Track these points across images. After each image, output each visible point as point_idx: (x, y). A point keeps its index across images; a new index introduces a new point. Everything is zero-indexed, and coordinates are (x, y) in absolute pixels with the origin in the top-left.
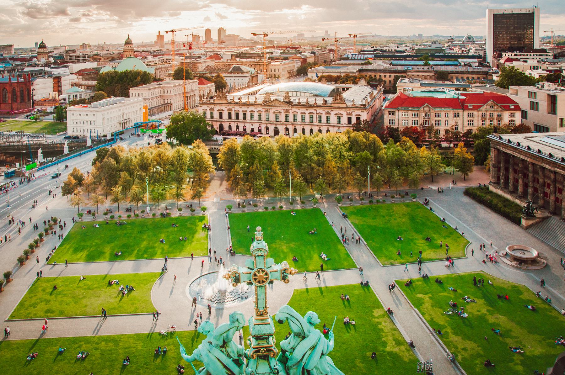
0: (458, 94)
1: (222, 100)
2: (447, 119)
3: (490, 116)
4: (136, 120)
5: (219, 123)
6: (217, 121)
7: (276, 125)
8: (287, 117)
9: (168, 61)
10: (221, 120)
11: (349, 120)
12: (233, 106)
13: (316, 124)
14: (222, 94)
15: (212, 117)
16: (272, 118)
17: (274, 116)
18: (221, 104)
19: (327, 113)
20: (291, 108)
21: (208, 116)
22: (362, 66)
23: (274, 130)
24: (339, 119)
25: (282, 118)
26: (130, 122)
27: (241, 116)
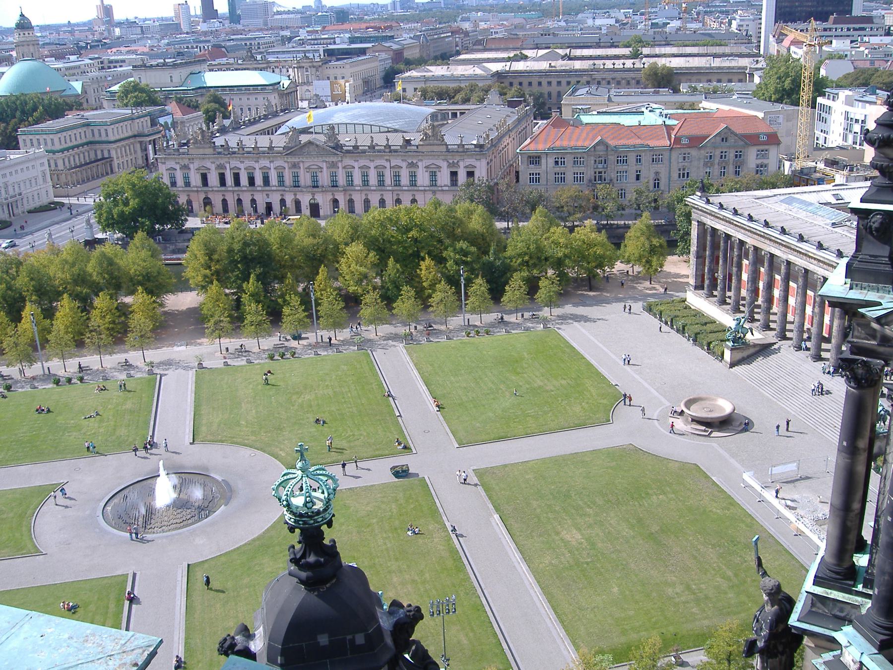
0: (666, 115)
1: (204, 148)
2: (638, 167)
3: (721, 157)
4: (36, 197)
5: (202, 196)
6: (197, 191)
7: (313, 194)
8: (334, 176)
9: (112, 65)
10: (205, 189)
11: (454, 174)
12: (227, 160)
13: (390, 188)
14: (203, 136)
15: (187, 184)
16: (305, 179)
17: (308, 176)
18: (203, 157)
19: (412, 165)
20: (340, 159)
21: (180, 182)
22: (504, 64)
23: (311, 204)
24: (433, 175)
25: (324, 178)
26: (25, 200)
27: (244, 180)
